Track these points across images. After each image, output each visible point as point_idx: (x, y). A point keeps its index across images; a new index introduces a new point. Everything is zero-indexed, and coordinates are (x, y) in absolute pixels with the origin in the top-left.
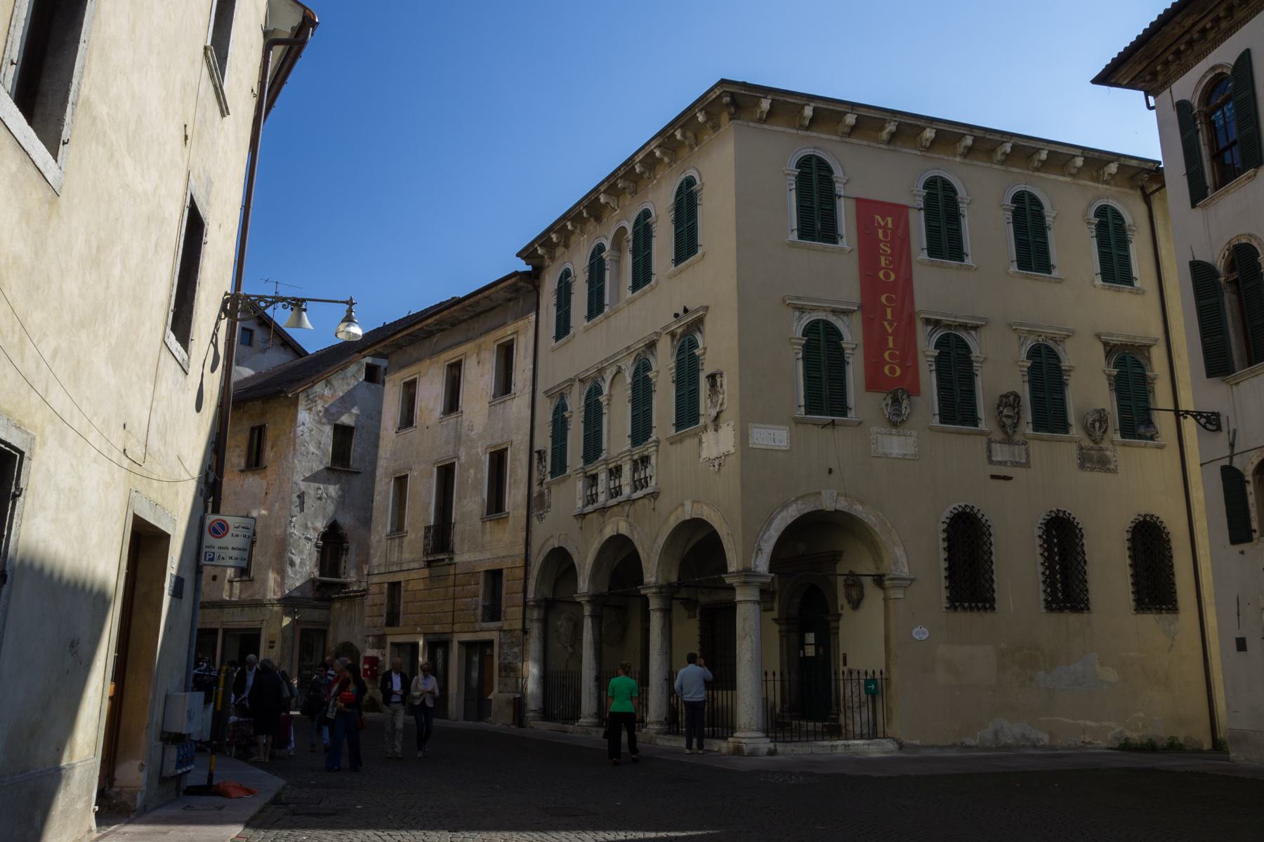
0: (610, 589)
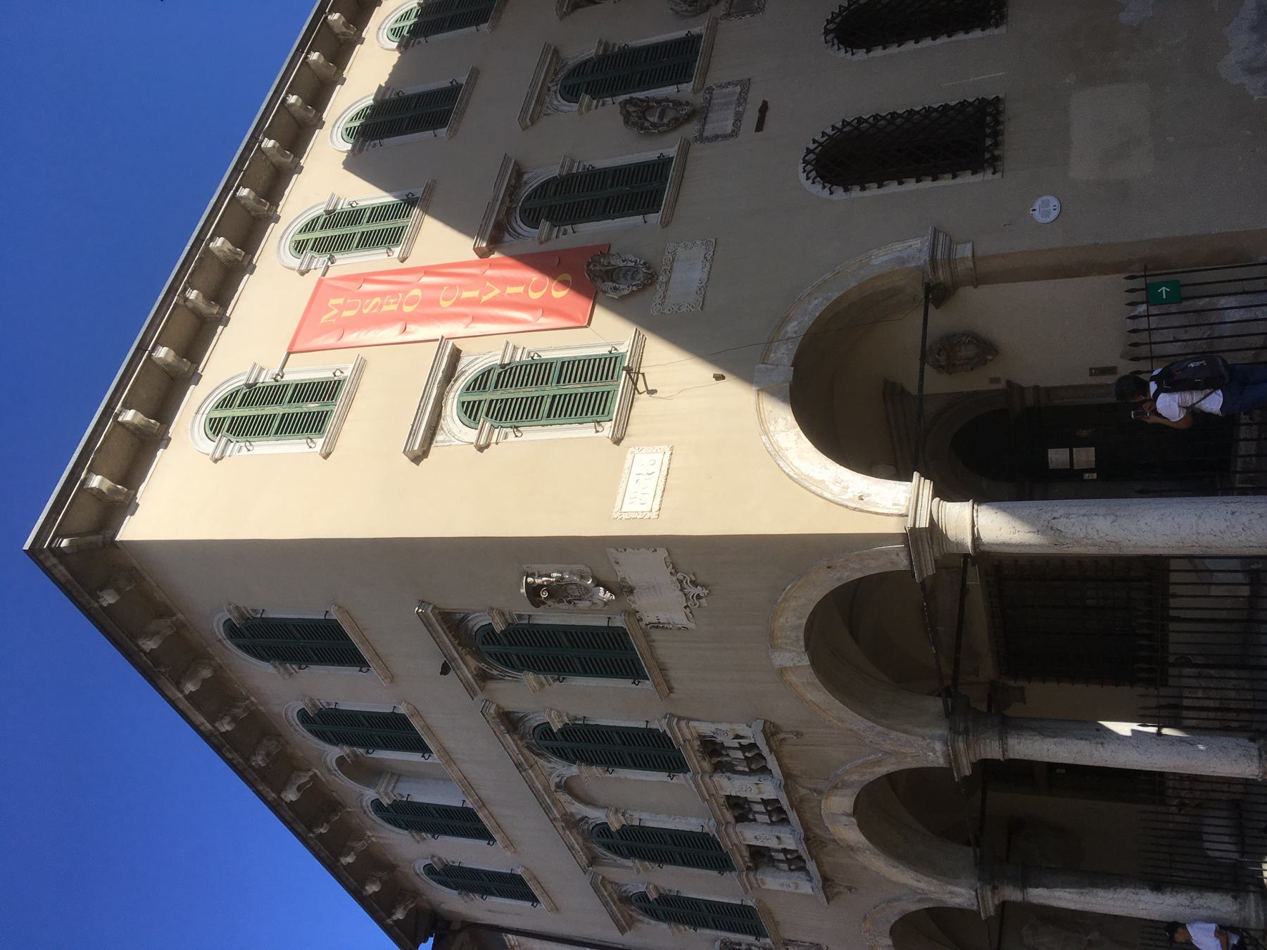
0: (968, 843)
